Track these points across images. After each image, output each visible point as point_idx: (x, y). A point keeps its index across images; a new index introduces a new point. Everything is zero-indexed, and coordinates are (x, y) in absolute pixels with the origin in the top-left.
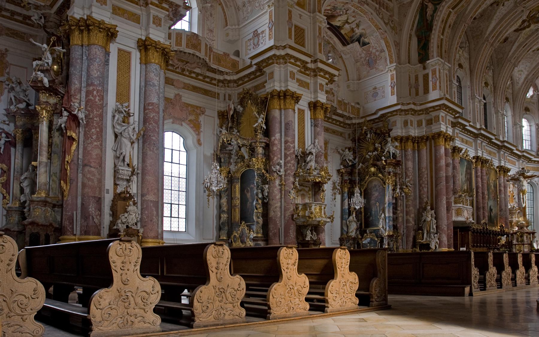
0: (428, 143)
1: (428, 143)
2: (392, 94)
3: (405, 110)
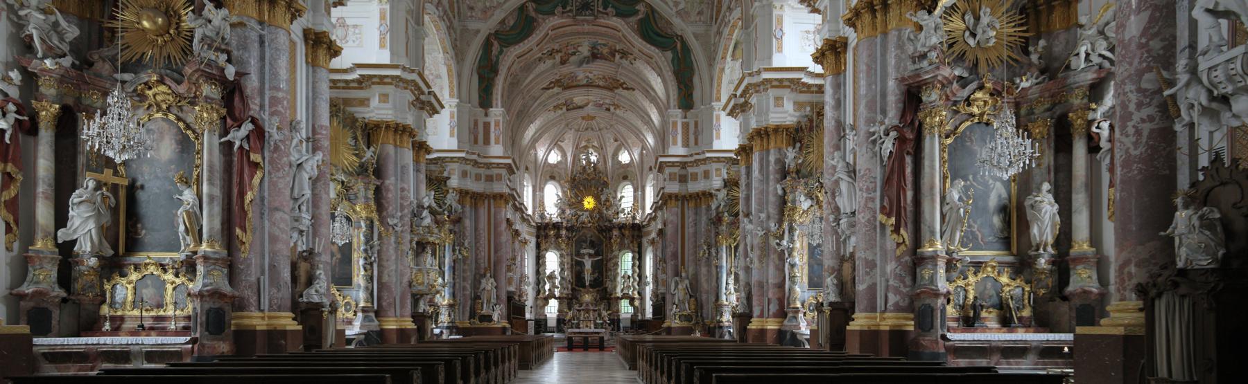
0: (486, 201)
1: (486, 201)
2: (452, 135)
3: (467, 160)
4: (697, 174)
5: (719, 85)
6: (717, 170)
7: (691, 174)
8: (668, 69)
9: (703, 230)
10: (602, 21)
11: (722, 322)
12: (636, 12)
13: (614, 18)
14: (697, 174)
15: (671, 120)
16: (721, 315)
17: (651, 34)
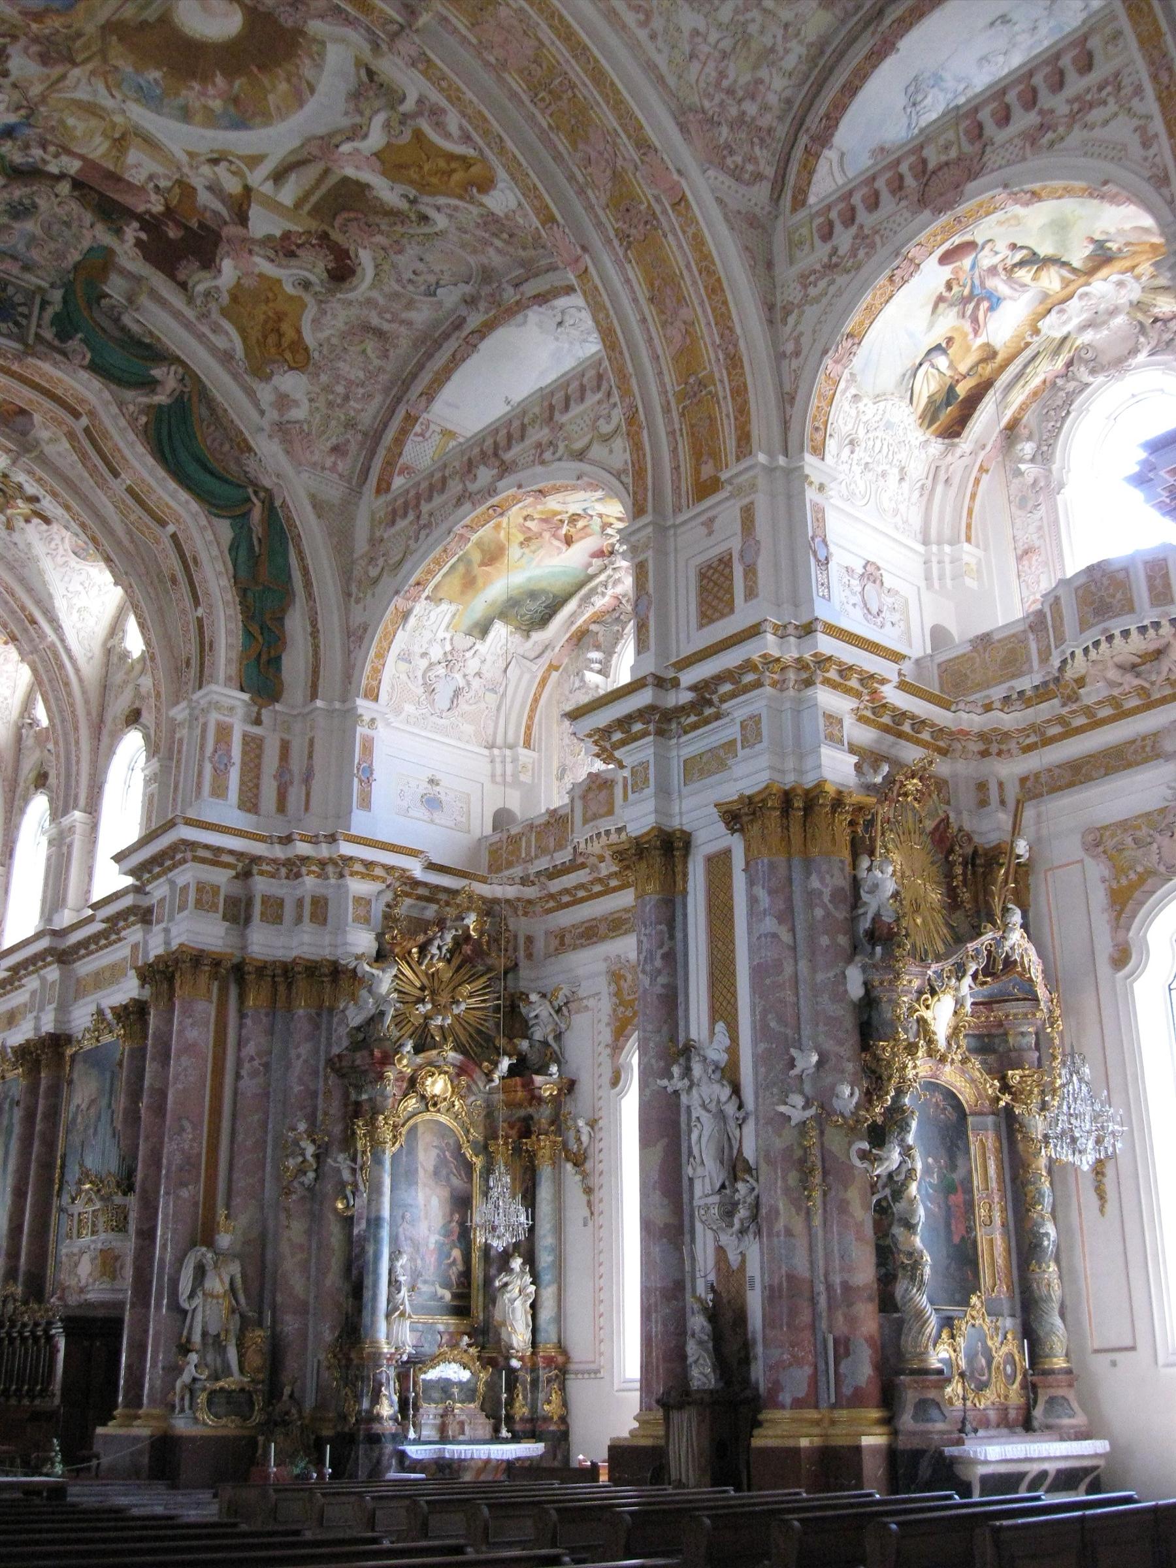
4: (281, 903)
5: (382, 656)
6: (358, 900)
7: (266, 900)
8: (220, 567)
9: (297, 1089)
10: (46, 367)
11: (378, 1418)
12: (151, 385)
13: (85, 375)
14: (281, 903)
15: (214, 717)
16: (376, 1398)
17: (183, 456)
